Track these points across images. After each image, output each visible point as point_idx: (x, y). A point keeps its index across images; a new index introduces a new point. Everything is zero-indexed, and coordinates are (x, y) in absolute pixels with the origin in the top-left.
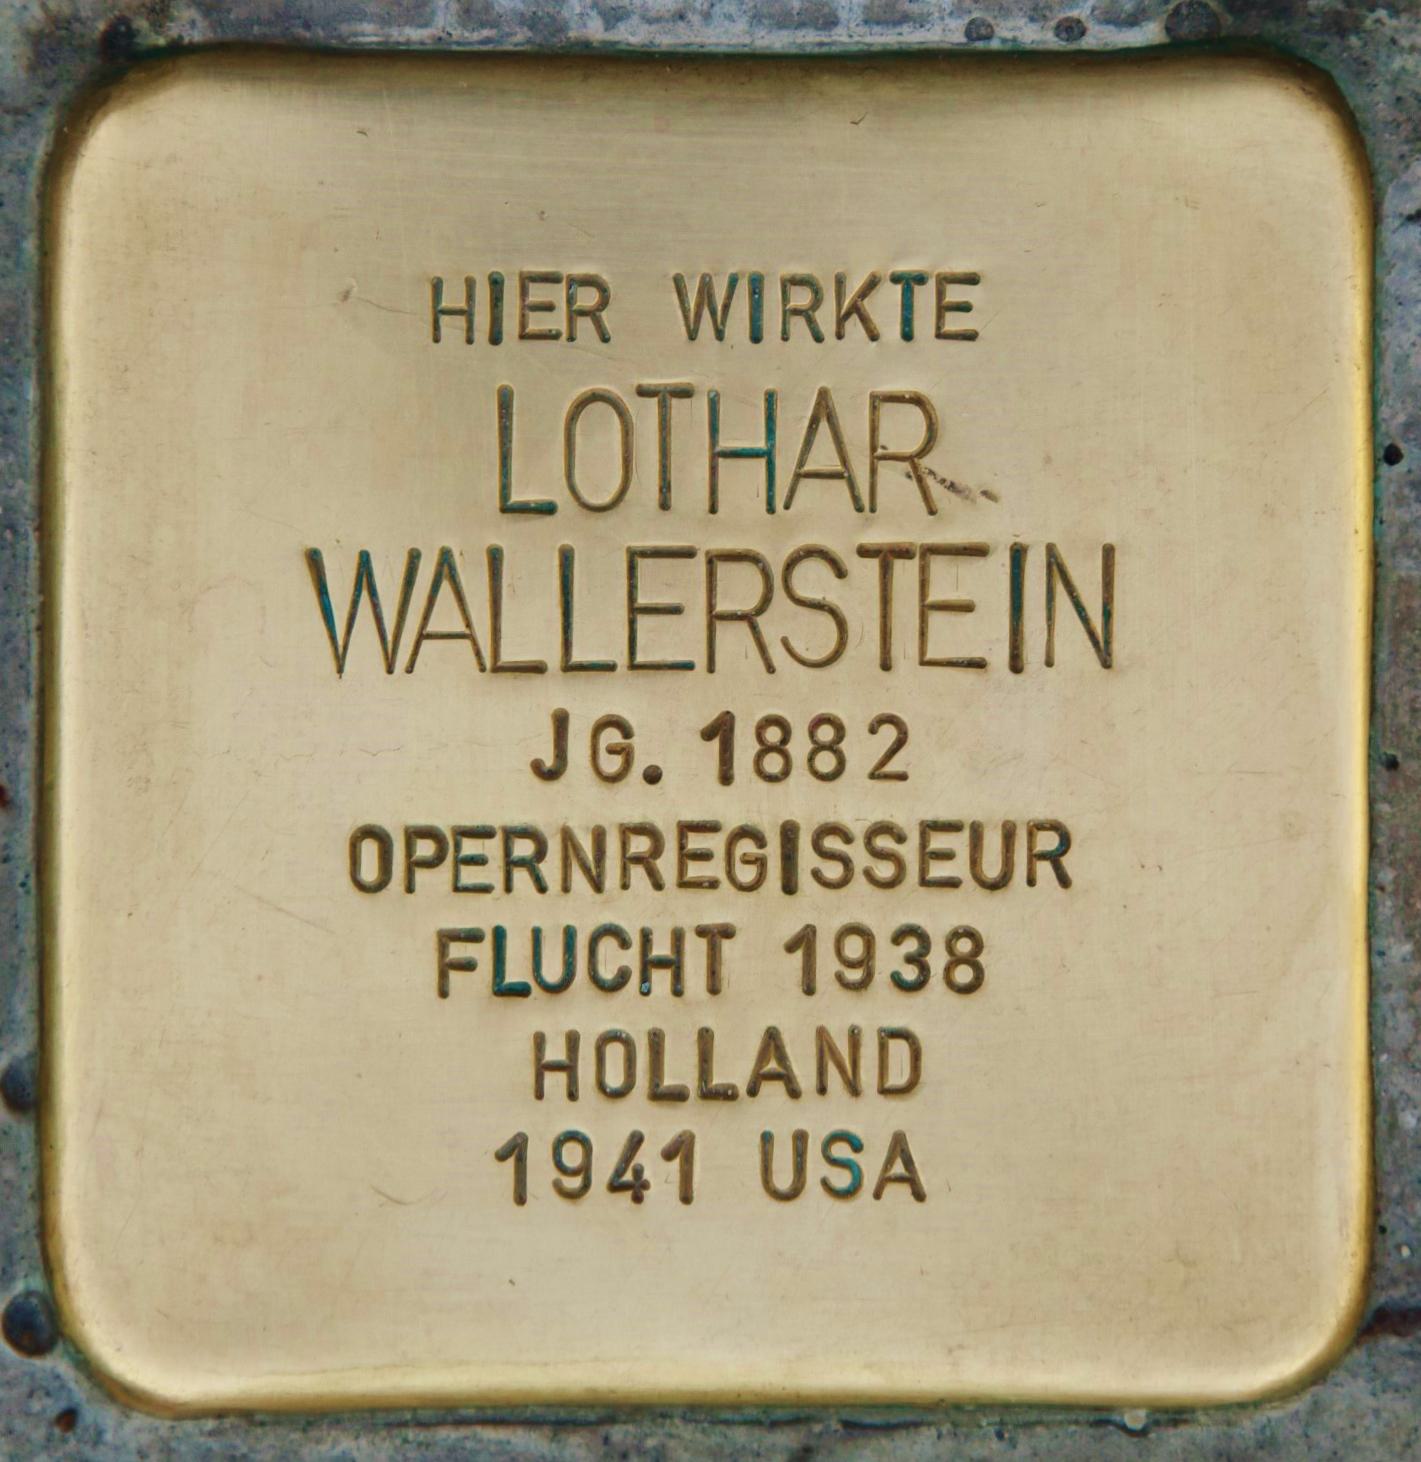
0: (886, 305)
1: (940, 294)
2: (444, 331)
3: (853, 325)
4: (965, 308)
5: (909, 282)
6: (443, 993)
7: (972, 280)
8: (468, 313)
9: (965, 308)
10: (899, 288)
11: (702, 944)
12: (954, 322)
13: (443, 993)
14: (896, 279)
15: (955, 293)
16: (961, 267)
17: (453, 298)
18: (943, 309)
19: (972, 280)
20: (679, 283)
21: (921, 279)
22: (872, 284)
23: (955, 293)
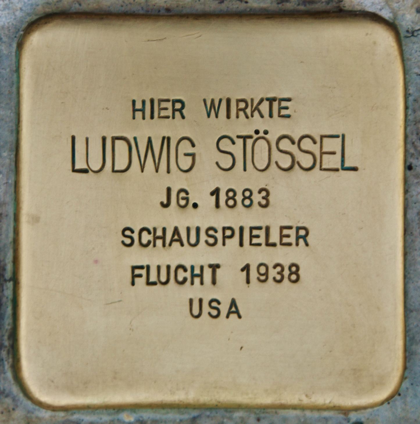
0: (265, 107)
1: (279, 104)
2: (136, 116)
3: (256, 113)
4: (287, 108)
5: (271, 100)
6: (133, 284)
7: (289, 100)
8: (143, 110)
9: (287, 108)
10: (268, 103)
11: (210, 270)
12: (284, 112)
13: (133, 284)
14: (268, 99)
15: (284, 104)
16: (286, 96)
17: (139, 106)
18: (280, 108)
19: (289, 100)
20: (205, 101)
21: (274, 99)
22: (262, 101)
23: (284, 104)
